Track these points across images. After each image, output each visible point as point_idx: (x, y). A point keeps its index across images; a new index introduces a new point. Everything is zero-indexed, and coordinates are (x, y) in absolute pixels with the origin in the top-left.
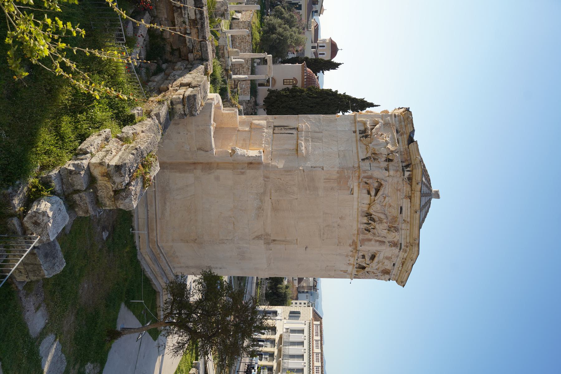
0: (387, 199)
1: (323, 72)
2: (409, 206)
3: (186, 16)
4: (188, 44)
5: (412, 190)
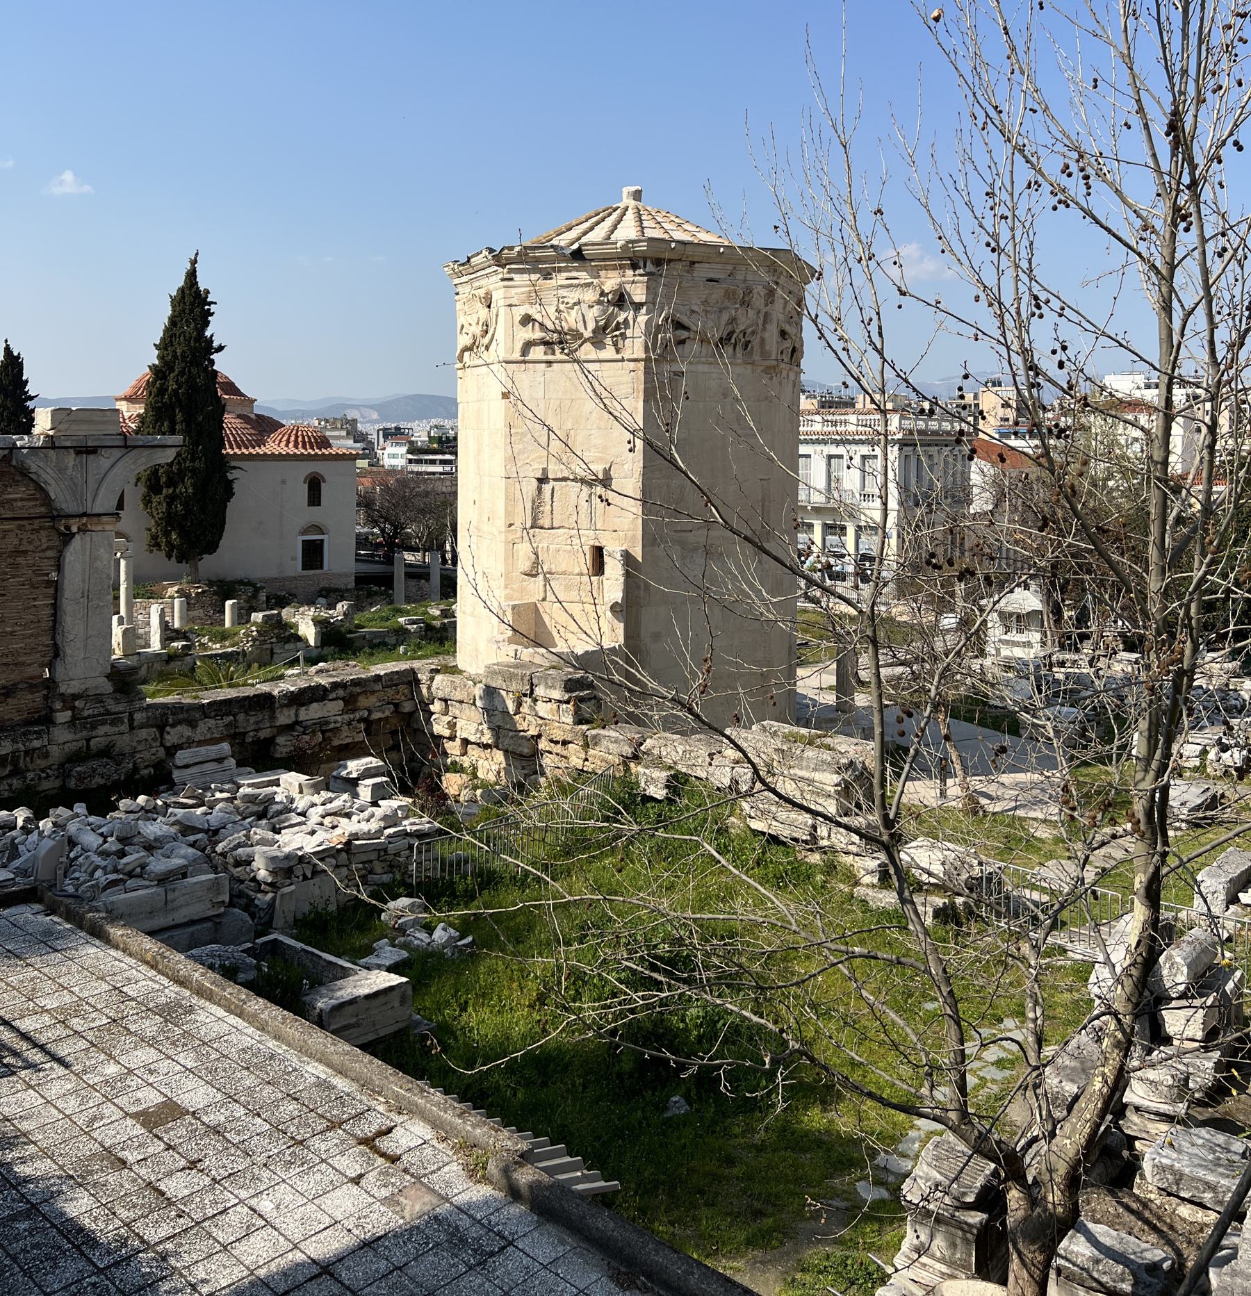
0: (695, 308)
1: (32, 398)
2: (707, 265)
3: (339, 718)
4: (387, 713)
5: (680, 260)
